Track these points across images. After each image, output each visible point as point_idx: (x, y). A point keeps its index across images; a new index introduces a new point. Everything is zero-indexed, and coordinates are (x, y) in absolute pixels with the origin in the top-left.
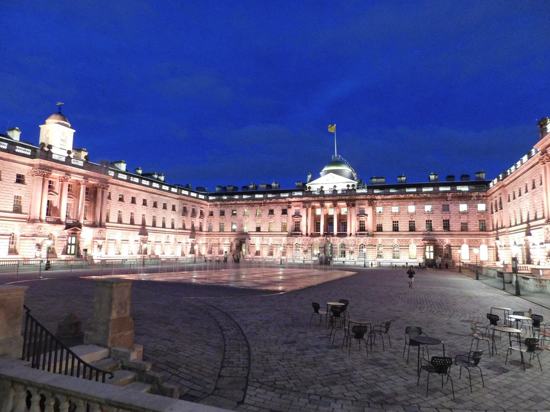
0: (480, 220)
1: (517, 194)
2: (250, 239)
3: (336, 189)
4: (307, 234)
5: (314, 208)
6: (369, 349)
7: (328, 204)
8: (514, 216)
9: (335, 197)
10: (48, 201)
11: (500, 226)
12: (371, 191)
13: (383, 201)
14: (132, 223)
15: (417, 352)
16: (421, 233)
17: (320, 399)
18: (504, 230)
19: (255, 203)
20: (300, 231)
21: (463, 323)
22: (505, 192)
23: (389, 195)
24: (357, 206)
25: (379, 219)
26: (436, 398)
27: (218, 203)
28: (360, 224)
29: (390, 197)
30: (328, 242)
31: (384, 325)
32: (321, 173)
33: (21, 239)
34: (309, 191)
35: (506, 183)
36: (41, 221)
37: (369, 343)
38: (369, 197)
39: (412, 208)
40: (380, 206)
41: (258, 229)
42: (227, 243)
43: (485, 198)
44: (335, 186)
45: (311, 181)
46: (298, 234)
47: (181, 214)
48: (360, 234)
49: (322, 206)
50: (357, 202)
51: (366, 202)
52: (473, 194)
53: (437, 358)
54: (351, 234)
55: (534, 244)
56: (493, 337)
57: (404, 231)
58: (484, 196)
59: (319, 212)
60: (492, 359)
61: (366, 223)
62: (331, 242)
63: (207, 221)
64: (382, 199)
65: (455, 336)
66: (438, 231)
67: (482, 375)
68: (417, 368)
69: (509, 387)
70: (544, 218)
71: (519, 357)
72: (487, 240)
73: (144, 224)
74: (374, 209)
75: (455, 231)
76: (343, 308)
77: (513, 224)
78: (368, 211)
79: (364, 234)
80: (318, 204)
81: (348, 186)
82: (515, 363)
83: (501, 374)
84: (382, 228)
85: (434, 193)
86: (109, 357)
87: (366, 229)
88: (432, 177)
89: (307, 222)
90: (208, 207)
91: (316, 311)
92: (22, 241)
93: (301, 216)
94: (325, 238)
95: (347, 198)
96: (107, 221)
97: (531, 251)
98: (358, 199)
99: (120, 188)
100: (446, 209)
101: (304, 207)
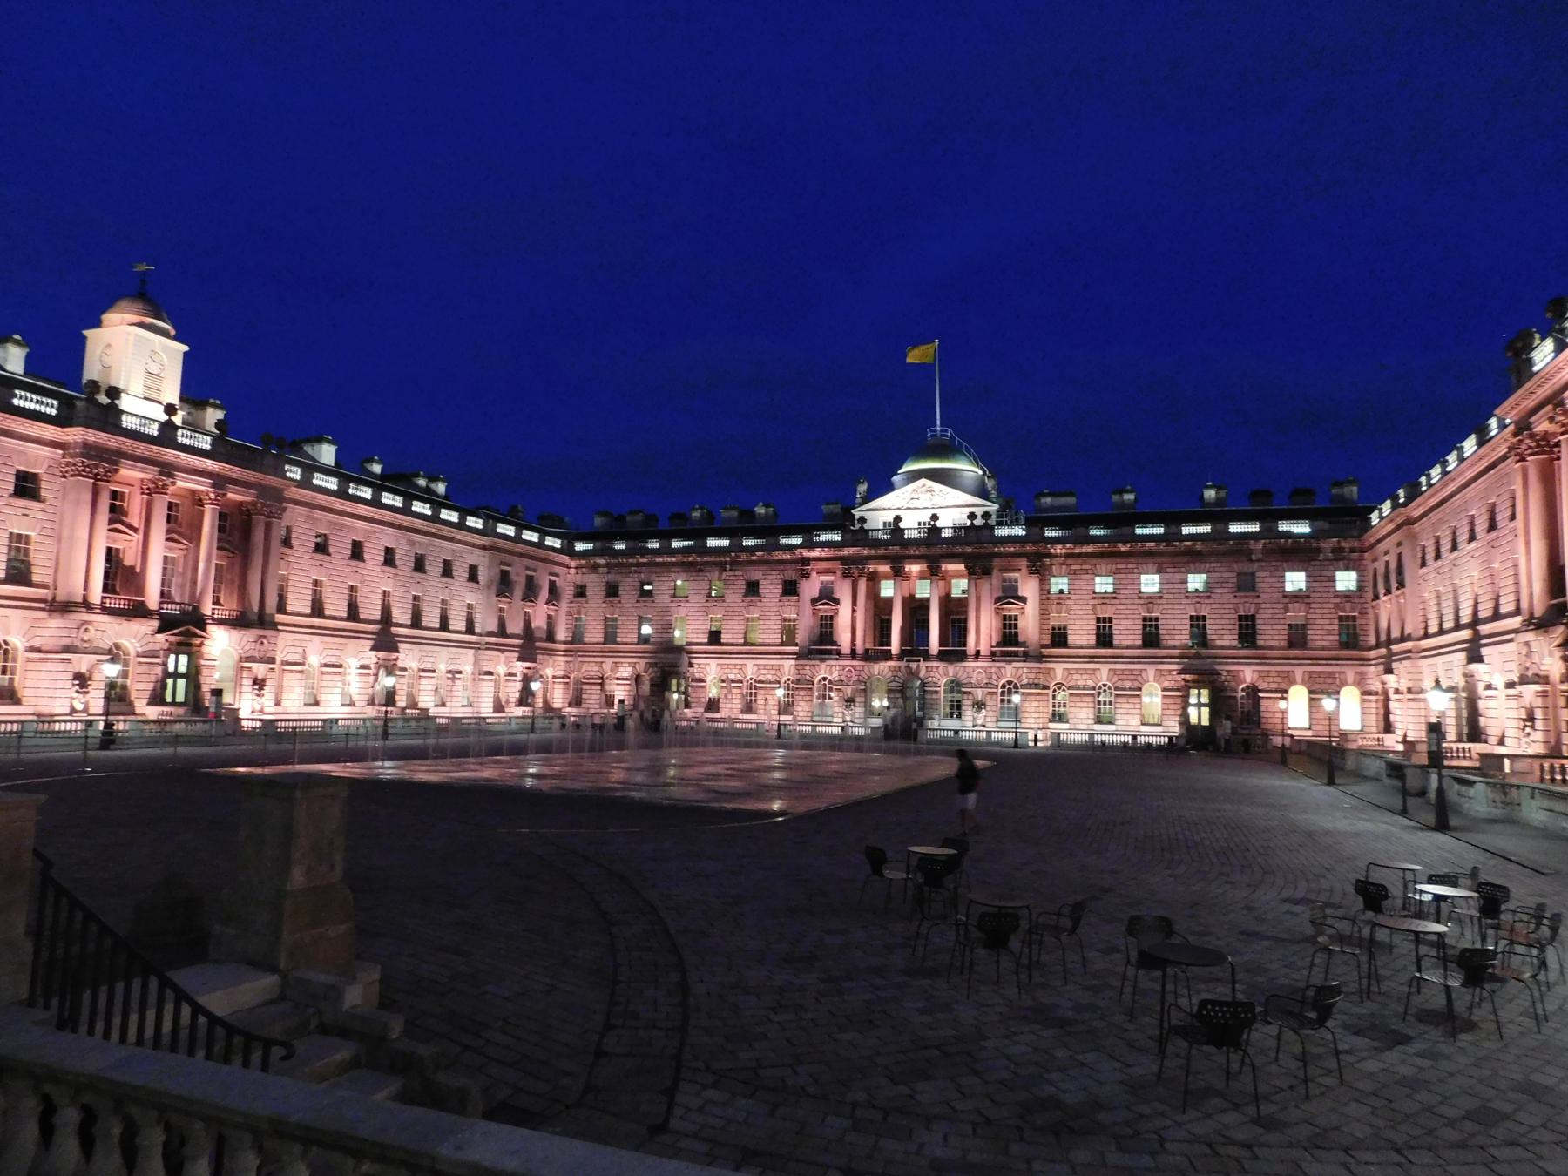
0: (1341, 618)
1: (1446, 545)
2: (691, 665)
3: (939, 524)
4: (853, 652)
5: (874, 579)
6: (1024, 977)
7: (914, 568)
8: (1435, 608)
9: (934, 548)
10: (109, 550)
11: (1395, 634)
12: (1037, 530)
13: (1069, 561)
14: (353, 613)
15: (1158, 987)
16: (1176, 652)
17: (885, 1119)
18: (1408, 645)
19: (707, 563)
20: (834, 643)
21: (1287, 906)
22: (1413, 537)
23: (1088, 543)
24: (995, 573)
25: (1059, 612)
26: (1209, 1116)
27: (602, 561)
28: (1004, 626)
29: (1089, 549)
30: (915, 675)
31: (1066, 911)
32: (895, 479)
33: (29, 660)
35: (1416, 514)
36: (88, 606)
37: (1025, 961)
38: (1029, 548)
39: (1150, 583)
40: (1061, 576)
41: (715, 637)
42: (626, 675)
43: (1355, 555)
45: (869, 498)
46: (829, 652)
47: (493, 591)
48: (1004, 654)
49: (898, 573)
50: (996, 562)
51: (1023, 562)
52: (1322, 545)
53: (1214, 1003)
54: (977, 655)
55: (1489, 687)
56: (1371, 945)
57: (1128, 647)
58: (1353, 550)
59: (887, 589)
60: (1368, 1007)
61: (1020, 624)
62: (922, 674)
63: (569, 613)
64: (1068, 556)
65: (1266, 943)
66: (1223, 647)
67: (1337, 1053)
68: (1157, 1032)
69: (1412, 1085)
70: (1517, 612)
71: (1441, 1001)
72: (1361, 673)
73: (386, 618)
74: (1044, 584)
75: (1271, 648)
76: (952, 864)
77: (1433, 629)
78: (1029, 588)
79: (1015, 654)
80: (885, 568)
81: (972, 516)
82: (1427, 1016)
83: (1390, 1048)
84: (1065, 636)
85: (1214, 540)
86: (282, 997)
87: (1021, 639)
88: (1210, 494)
89: (853, 619)
90: (573, 571)
91: (877, 869)
92: (31, 666)
93: (837, 601)
94: (904, 663)
95: (969, 549)
96: (282, 609)
97: (1481, 704)
98: (999, 555)
99: (318, 514)
100: (1246, 585)
101: (845, 575)
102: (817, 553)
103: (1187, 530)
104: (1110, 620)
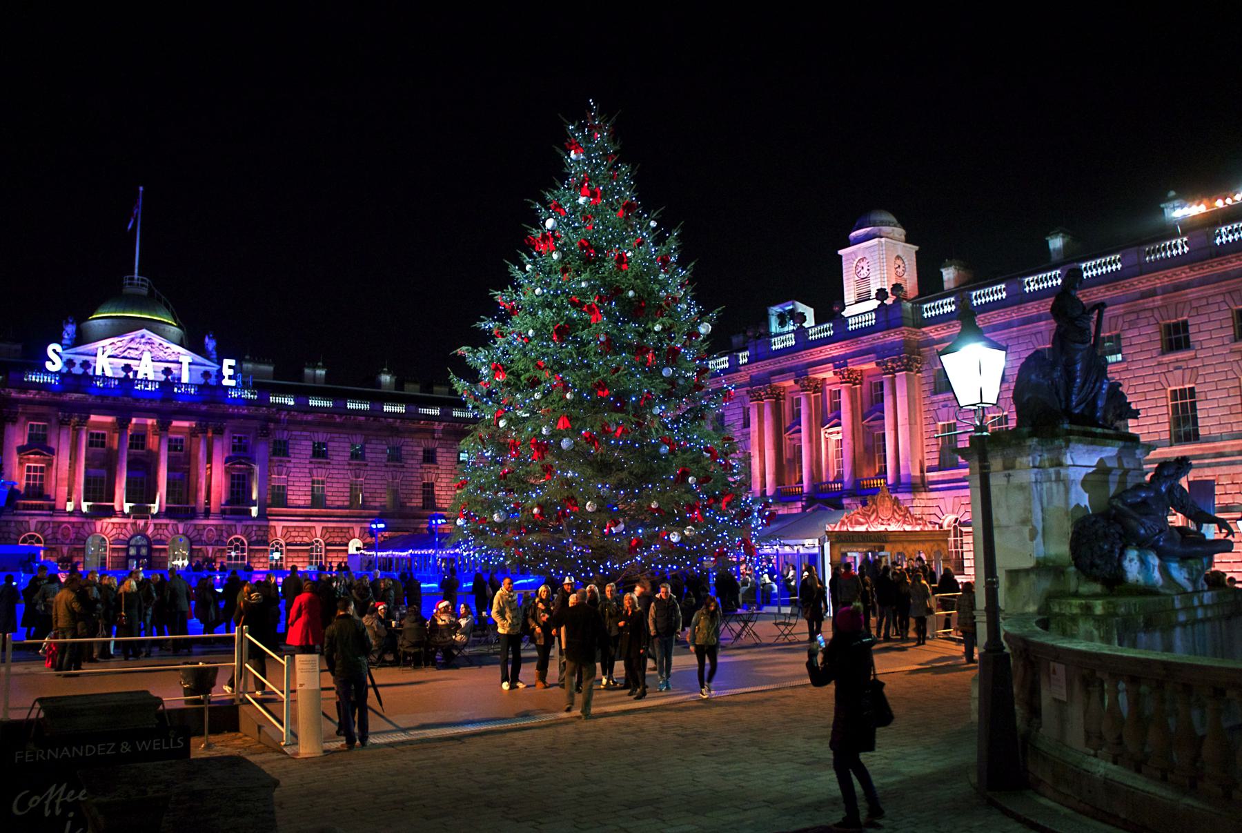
20: (48, 498)
24: (227, 431)
25: (280, 474)
28: (233, 485)
29: (310, 418)
34: (85, 373)
44: (127, 368)
48: (233, 512)
57: (339, 507)
93: (51, 451)
95: (204, 408)
101: (62, 423)
102: (31, 395)
103: (387, 408)
104: (323, 483)
